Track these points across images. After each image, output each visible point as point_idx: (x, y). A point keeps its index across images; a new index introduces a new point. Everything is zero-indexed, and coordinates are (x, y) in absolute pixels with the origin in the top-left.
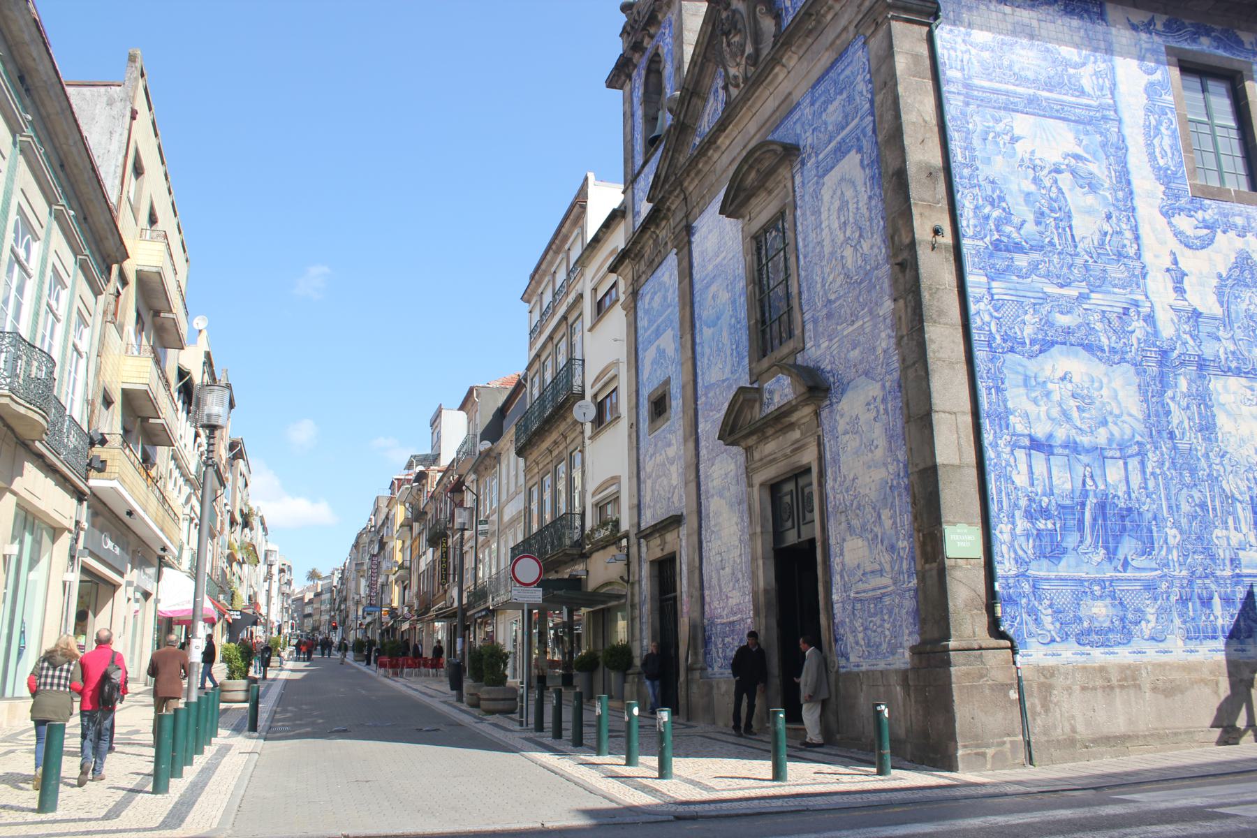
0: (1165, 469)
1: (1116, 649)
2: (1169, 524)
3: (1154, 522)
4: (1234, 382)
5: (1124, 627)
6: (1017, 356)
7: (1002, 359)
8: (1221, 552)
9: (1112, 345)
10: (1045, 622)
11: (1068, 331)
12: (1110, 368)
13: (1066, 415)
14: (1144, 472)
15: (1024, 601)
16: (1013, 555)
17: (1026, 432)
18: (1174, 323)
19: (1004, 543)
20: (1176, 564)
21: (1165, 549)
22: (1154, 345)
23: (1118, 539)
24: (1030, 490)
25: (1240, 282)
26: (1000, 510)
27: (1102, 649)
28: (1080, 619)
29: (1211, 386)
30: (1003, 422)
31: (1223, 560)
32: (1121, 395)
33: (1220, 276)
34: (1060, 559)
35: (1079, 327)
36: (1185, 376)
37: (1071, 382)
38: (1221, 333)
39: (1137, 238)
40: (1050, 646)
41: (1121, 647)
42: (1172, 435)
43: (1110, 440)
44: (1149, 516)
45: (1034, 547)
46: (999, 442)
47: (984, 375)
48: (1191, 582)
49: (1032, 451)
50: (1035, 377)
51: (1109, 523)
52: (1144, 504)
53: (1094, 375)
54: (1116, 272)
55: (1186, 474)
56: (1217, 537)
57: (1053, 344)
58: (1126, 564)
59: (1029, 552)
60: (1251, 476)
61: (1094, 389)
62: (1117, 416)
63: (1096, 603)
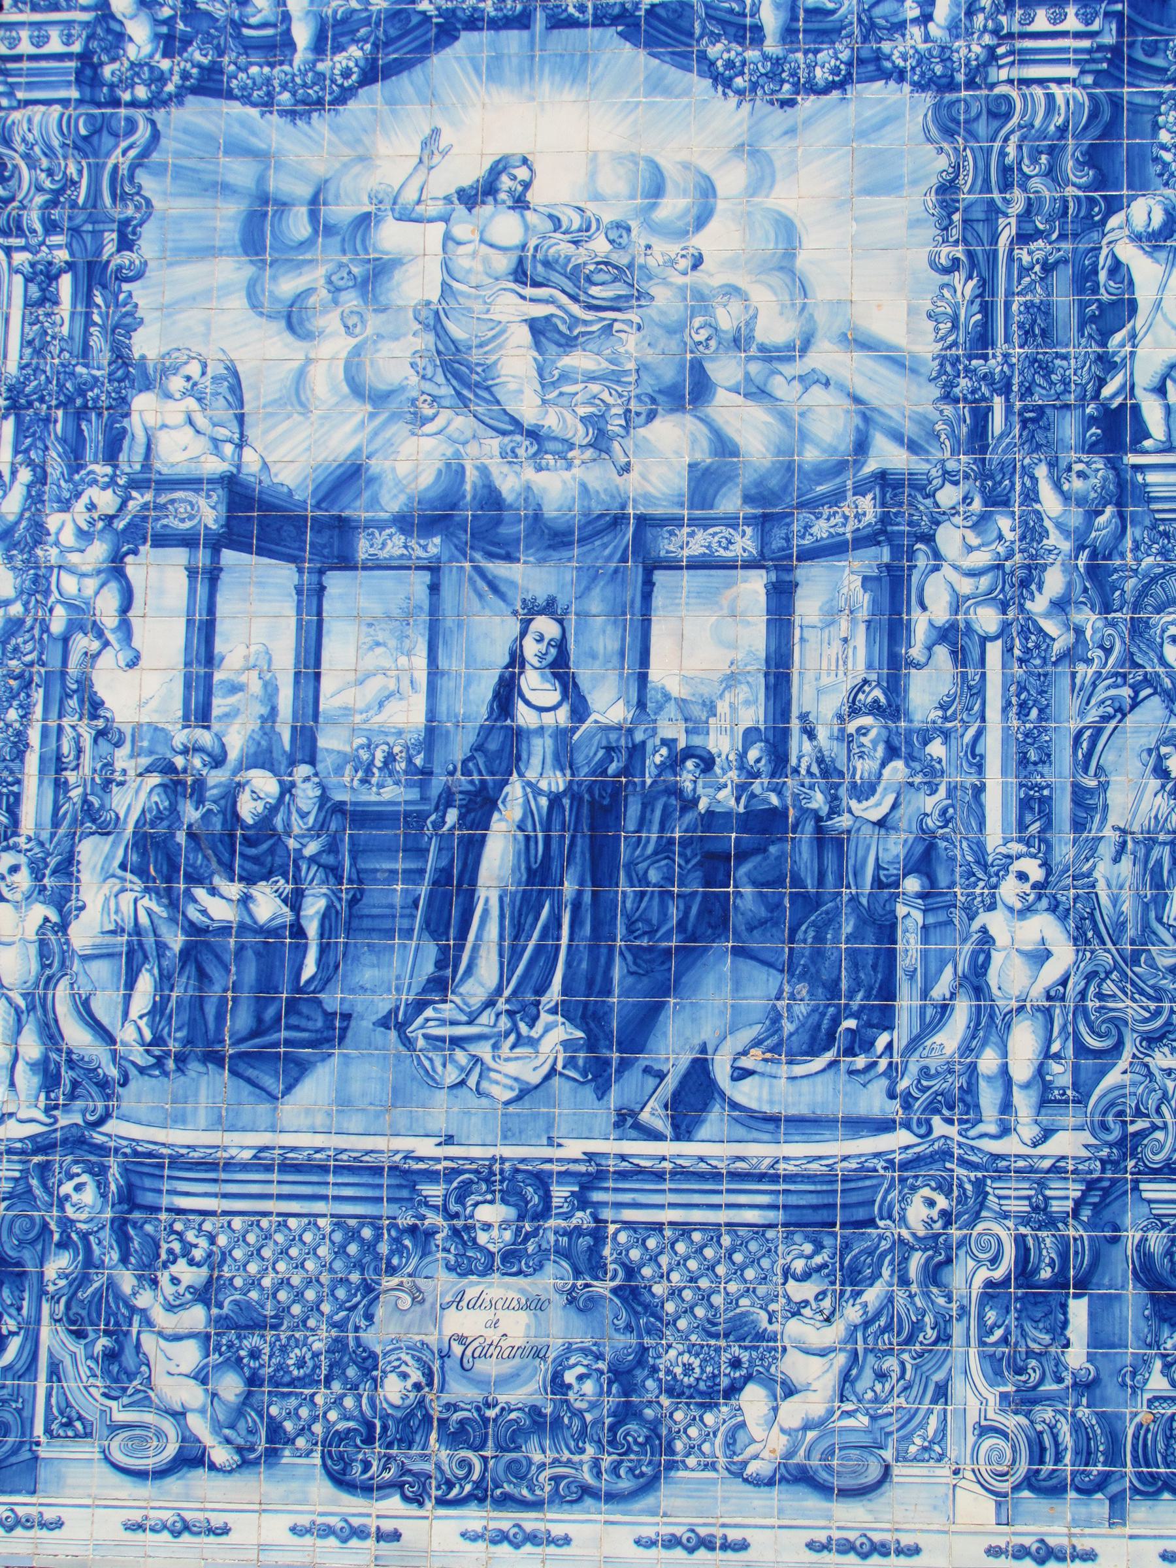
0: (1038, 605)
1: (556, 1521)
2: (1009, 890)
3: (912, 884)
5: (626, 1413)
6: (235, 108)
7: (143, 133)
10: (159, 1368)
12: (779, 118)
15: (58, 1265)
17: (214, 466)
20: (1023, 1102)
21: (962, 1010)
24: (180, 737)
27: (475, 1518)
28: (368, 1363)
30: (93, 430)
34: (297, 1071)
37: (520, 203)
40: (173, 1484)
44: (895, 847)
45: (158, 1011)
46: (53, 521)
47: (33, 218)
49: (229, 556)
51: (624, 888)
52: (865, 791)
59: (127, 1035)
62: (772, 356)
63: (474, 1287)
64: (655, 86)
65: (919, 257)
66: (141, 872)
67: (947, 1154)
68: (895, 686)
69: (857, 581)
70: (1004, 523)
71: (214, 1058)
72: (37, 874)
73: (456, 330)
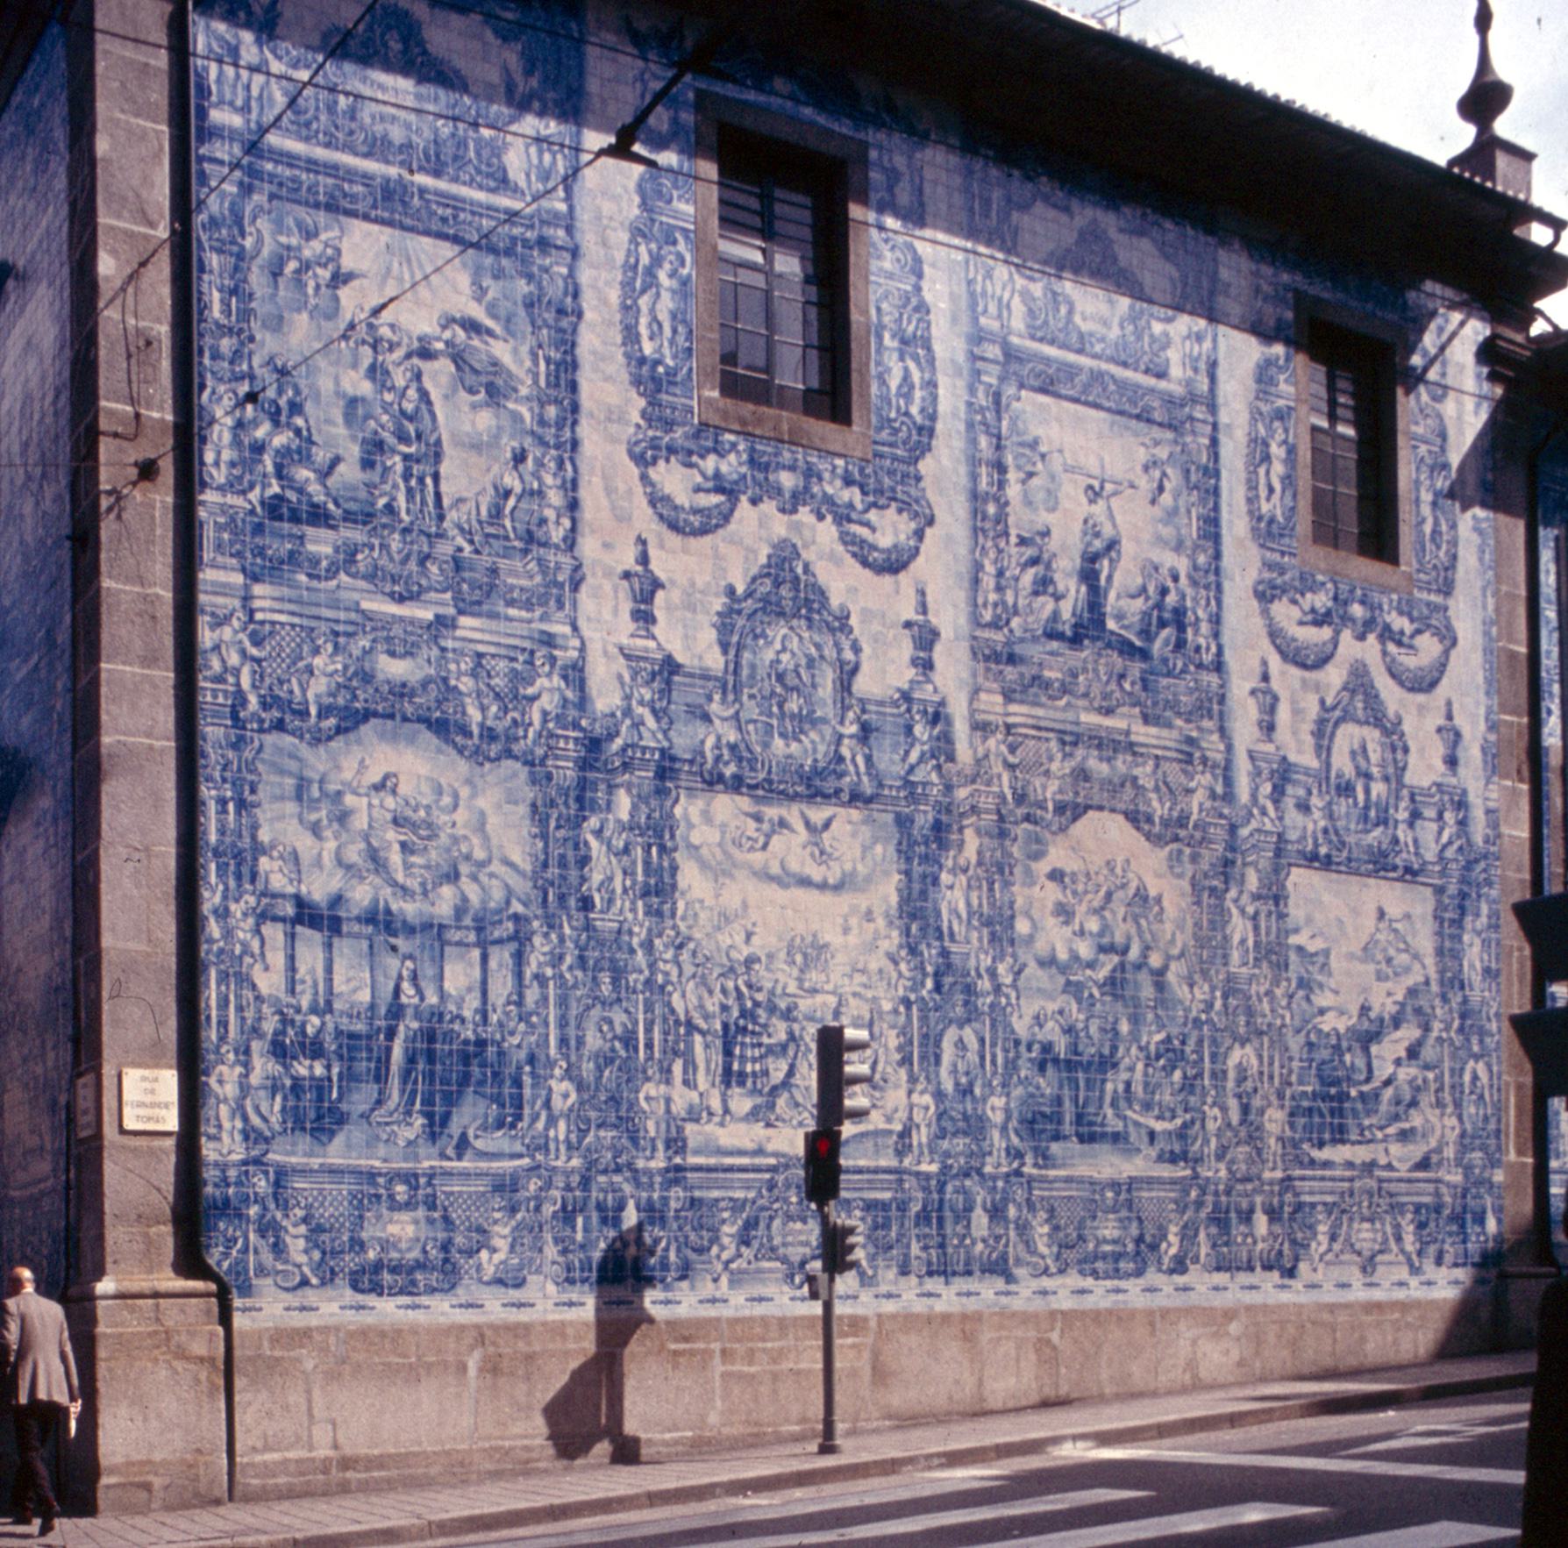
0: (564, 967)
1: (424, 1300)
2: (557, 1072)
3: (527, 1069)
4: (726, 806)
8: (651, 1125)
9: (489, 723)
11: (402, 691)
13: (376, 859)
14: (519, 975)
15: (253, 1211)
16: (239, 1124)
18: (622, 684)
19: (226, 1100)
20: (563, 1148)
22: (576, 726)
23: (451, 1100)
25: (771, 608)
26: (223, 1038)
29: (678, 811)
31: (653, 1140)
32: (493, 821)
33: (731, 591)
34: (332, 1134)
35: (425, 684)
36: (629, 791)
37: (394, 792)
38: (715, 708)
39: (573, 505)
40: (299, 1292)
41: (438, 1296)
42: (586, 904)
43: (460, 911)
45: (283, 1110)
48: (586, 1183)
49: (299, 929)
50: (321, 782)
51: (438, 1067)
52: (512, 1033)
53: (443, 781)
54: (520, 574)
55: (605, 978)
56: (648, 1098)
57: (367, 715)
58: (463, 1145)
59: (273, 1119)
60: (730, 985)
61: (441, 809)
62: (482, 865)
63: (396, 1216)
64: (439, 751)
65: (525, 832)
66: (274, 1054)
67: (538, 1167)
68: (521, 995)
69: (507, 955)
70: (553, 936)
71: (303, 1129)
72: (236, 1052)
73: (375, 843)
